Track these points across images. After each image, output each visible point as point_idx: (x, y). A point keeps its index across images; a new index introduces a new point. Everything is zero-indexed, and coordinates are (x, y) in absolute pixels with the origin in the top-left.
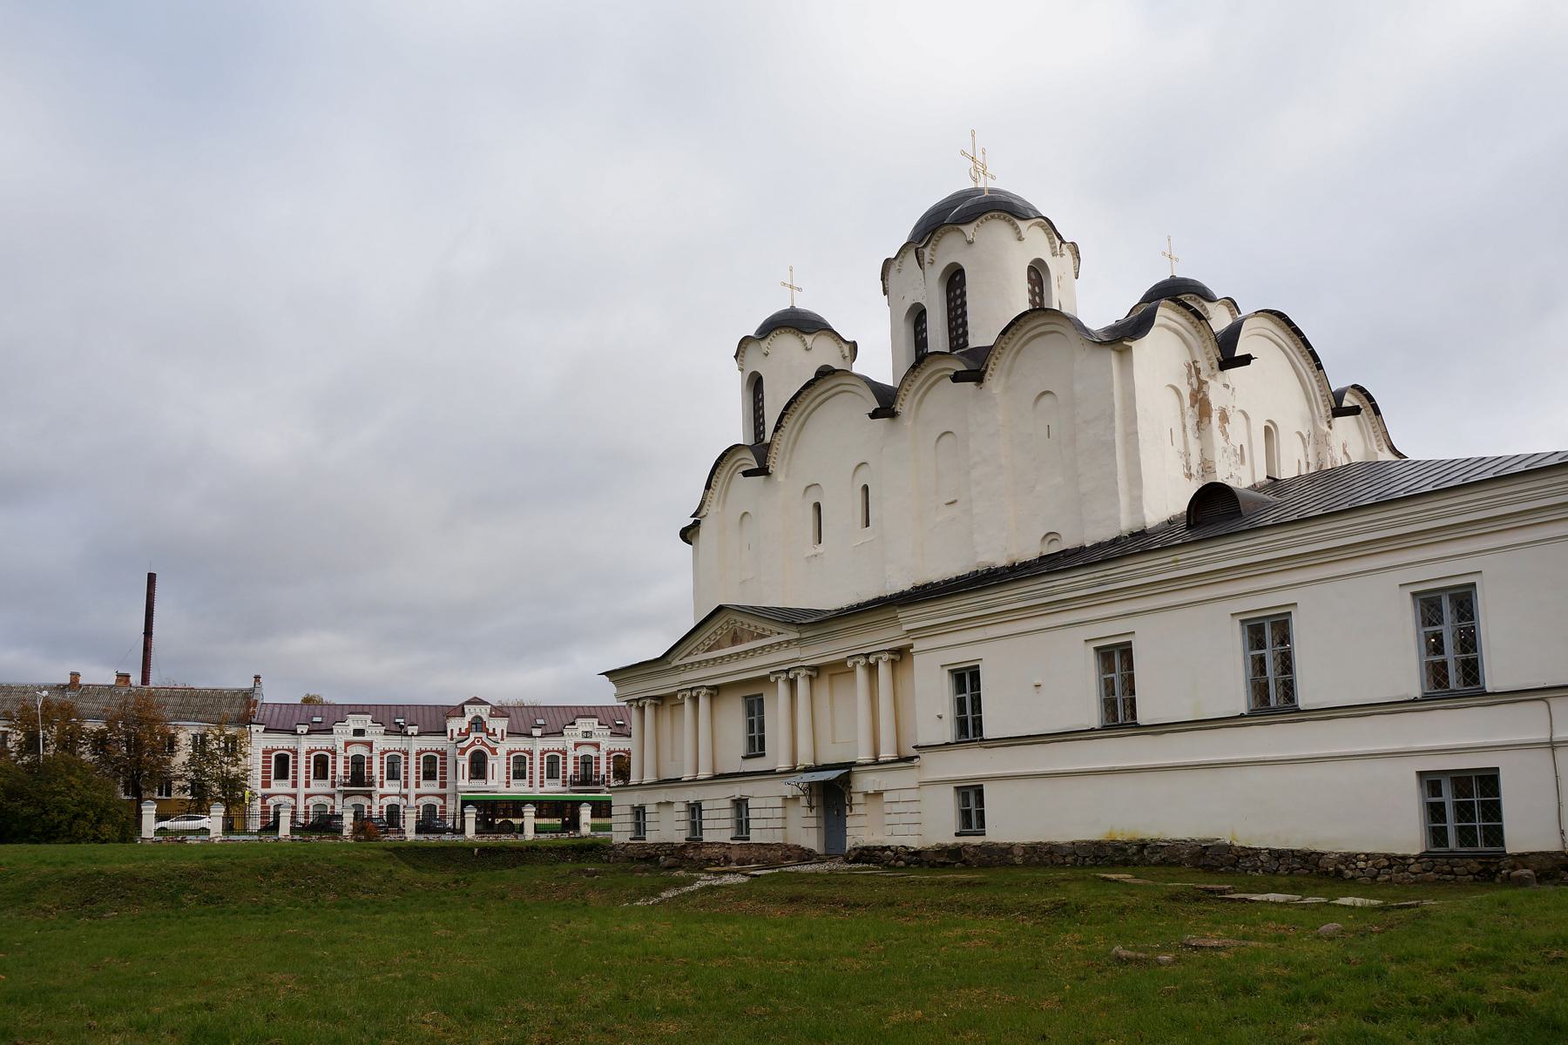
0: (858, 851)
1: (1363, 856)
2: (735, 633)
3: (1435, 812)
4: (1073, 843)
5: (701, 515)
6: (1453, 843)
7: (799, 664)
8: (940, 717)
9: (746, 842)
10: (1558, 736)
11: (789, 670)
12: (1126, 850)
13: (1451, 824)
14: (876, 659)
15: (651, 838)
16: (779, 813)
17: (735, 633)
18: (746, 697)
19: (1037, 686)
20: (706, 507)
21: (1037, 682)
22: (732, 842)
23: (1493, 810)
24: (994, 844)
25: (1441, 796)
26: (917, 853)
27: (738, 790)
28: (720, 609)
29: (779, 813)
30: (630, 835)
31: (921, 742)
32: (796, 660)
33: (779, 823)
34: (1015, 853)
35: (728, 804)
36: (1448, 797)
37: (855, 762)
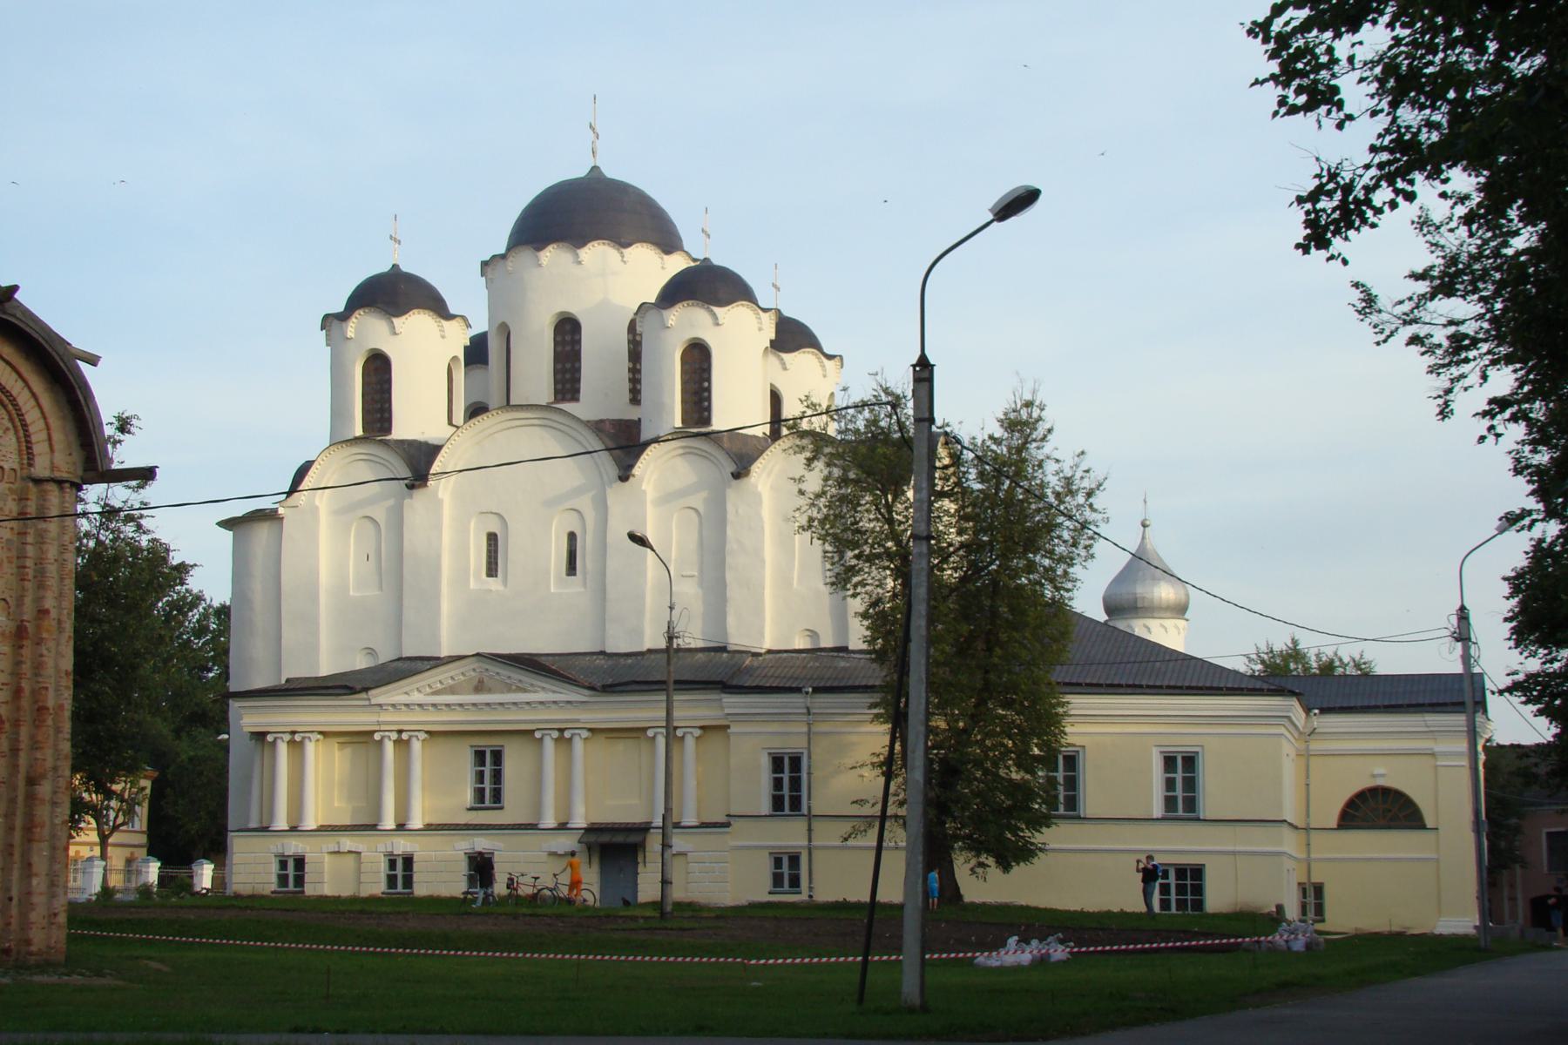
2: (481, 682)
6: (1174, 910)
13: (1173, 897)
23: (1198, 890)
32: (578, 721)
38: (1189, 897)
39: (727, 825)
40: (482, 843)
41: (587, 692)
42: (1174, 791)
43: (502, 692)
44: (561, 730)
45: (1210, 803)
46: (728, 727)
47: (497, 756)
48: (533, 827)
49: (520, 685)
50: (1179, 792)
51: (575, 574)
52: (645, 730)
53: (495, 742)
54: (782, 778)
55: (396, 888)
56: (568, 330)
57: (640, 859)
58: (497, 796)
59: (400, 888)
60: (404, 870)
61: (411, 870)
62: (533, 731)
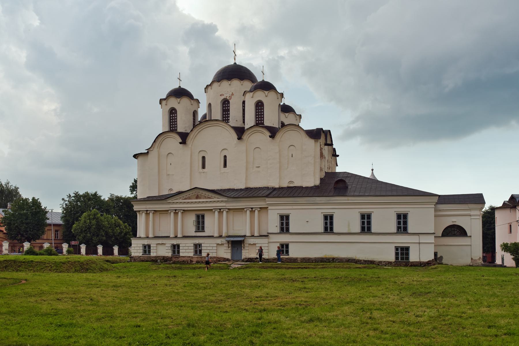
0: (247, 259)
2: (198, 195)
3: (397, 254)
4: (315, 258)
5: (149, 150)
7: (225, 208)
8: (277, 226)
9: (201, 256)
10: (421, 242)
11: (221, 209)
12: (329, 260)
13: (400, 256)
14: (255, 210)
15: (153, 254)
16: (215, 248)
17: (198, 195)
18: (196, 214)
19: (308, 221)
20: (152, 148)
21: (307, 221)
22: (193, 256)
23: (408, 254)
24: (292, 258)
25: (398, 251)
26: (267, 259)
27: (197, 241)
28: (196, 188)
29: (215, 248)
30: (142, 253)
31: (269, 232)
33: (215, 251)
34: (298, 260)
35: (192, 245)
36: (399, 251)
37: (246, 235)
39: (268, 236)
40: (197, 241)
41: (227, 198)
42: (400, 225)
43: (204, 199)
44: (220, 209)
45: (411, 229)
46: (268, 207)
47: (203, 217)
48: (212, 237)
49: (209, 196)
50: (402, 225)
51: (226, 167)
52: (243, 209)
54: (283, 222)
56: (226, 103)
57: (243, 245)
58: (203, 228)
59: (176, 254)
61: (179, 249)
62: (212, 210)
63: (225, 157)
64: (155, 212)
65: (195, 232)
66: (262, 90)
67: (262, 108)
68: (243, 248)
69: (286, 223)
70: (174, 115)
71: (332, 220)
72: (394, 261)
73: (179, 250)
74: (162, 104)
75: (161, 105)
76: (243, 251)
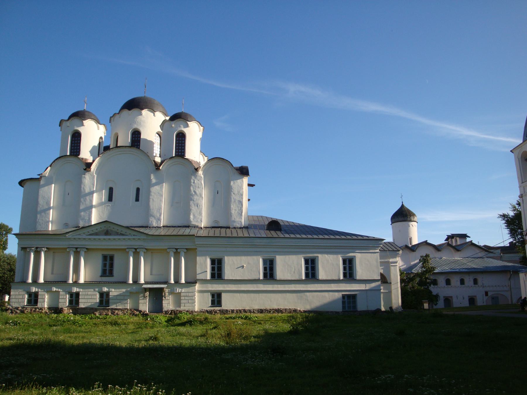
1: (330, 312)
2: (107, 231)
3: (343, 303)
13: (347, 305)
18: (102, 254)
28: (106, 221)
38: (352, 305)
43: (115, 235)
46: (196, 249)
47: (112, 258)
53: (111, 253)
55: (73, 304)
60: (76, 298)
62: (125, 249)
63: (138, 190)
64: (47, 250)
65: (101, 276)
66: (185, 121)
67: (183, 139)
68: (164, 298)
69: (218, 267)
70: (76, 139)
71: (272, 265)
72: (341, 311)
73: (79, 300)
74: (62, 126)
75: (61, 128)
76: (164, 302)
